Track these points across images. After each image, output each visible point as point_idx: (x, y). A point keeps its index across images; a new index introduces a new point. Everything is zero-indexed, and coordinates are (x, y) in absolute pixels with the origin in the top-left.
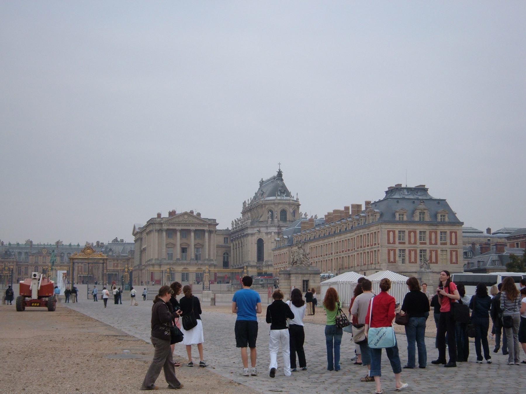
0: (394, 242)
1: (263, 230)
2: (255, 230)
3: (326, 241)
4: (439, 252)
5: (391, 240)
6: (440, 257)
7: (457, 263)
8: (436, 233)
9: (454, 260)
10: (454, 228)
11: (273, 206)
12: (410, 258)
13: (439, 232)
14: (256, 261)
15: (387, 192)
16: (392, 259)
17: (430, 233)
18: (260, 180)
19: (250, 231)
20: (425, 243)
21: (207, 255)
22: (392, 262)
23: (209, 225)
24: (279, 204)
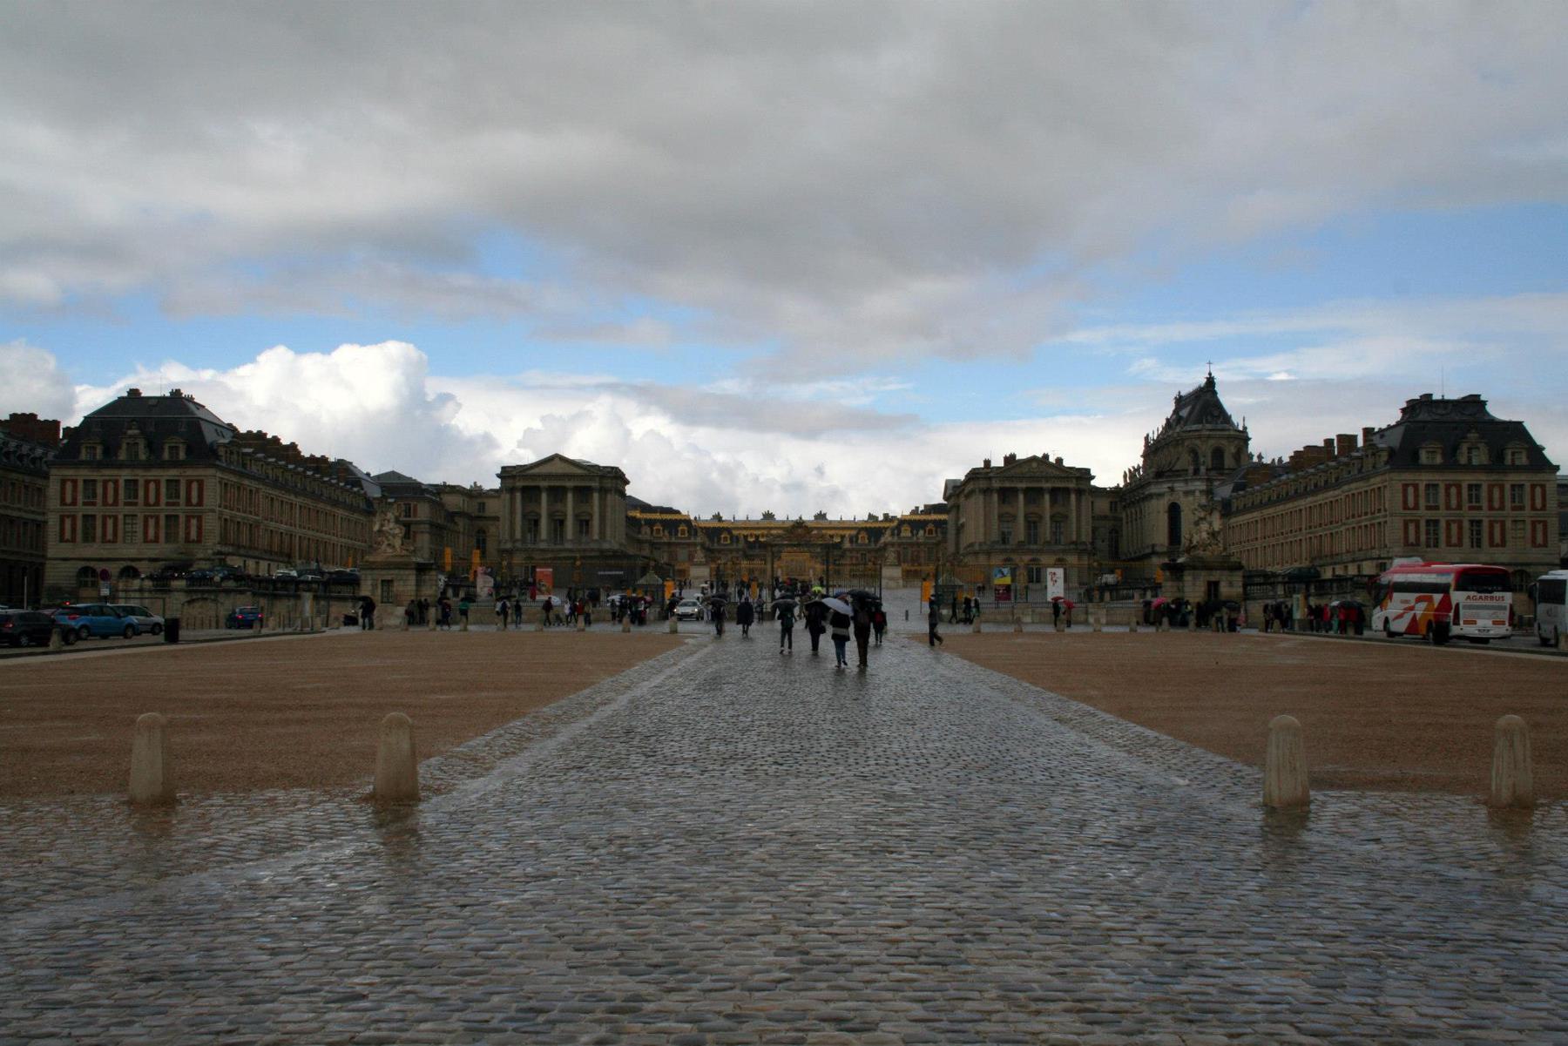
0: (1416, 507)
2: (1164, 488)
3: (1290, 505)
4: (1509, 524)
6: (1508, 537)
8: (1502, 488)
9: (1540, 539)
10: (1538, 477)
11: (1198, 442)
12: (1449, 536)
13: (1508, 487)
16: (1412, 539)
17: (1490, 488)
18: (1175, 394)
19: (1154, 489)
20: (1480, 508)
23: (1078, 479)
24: (1209, 437)
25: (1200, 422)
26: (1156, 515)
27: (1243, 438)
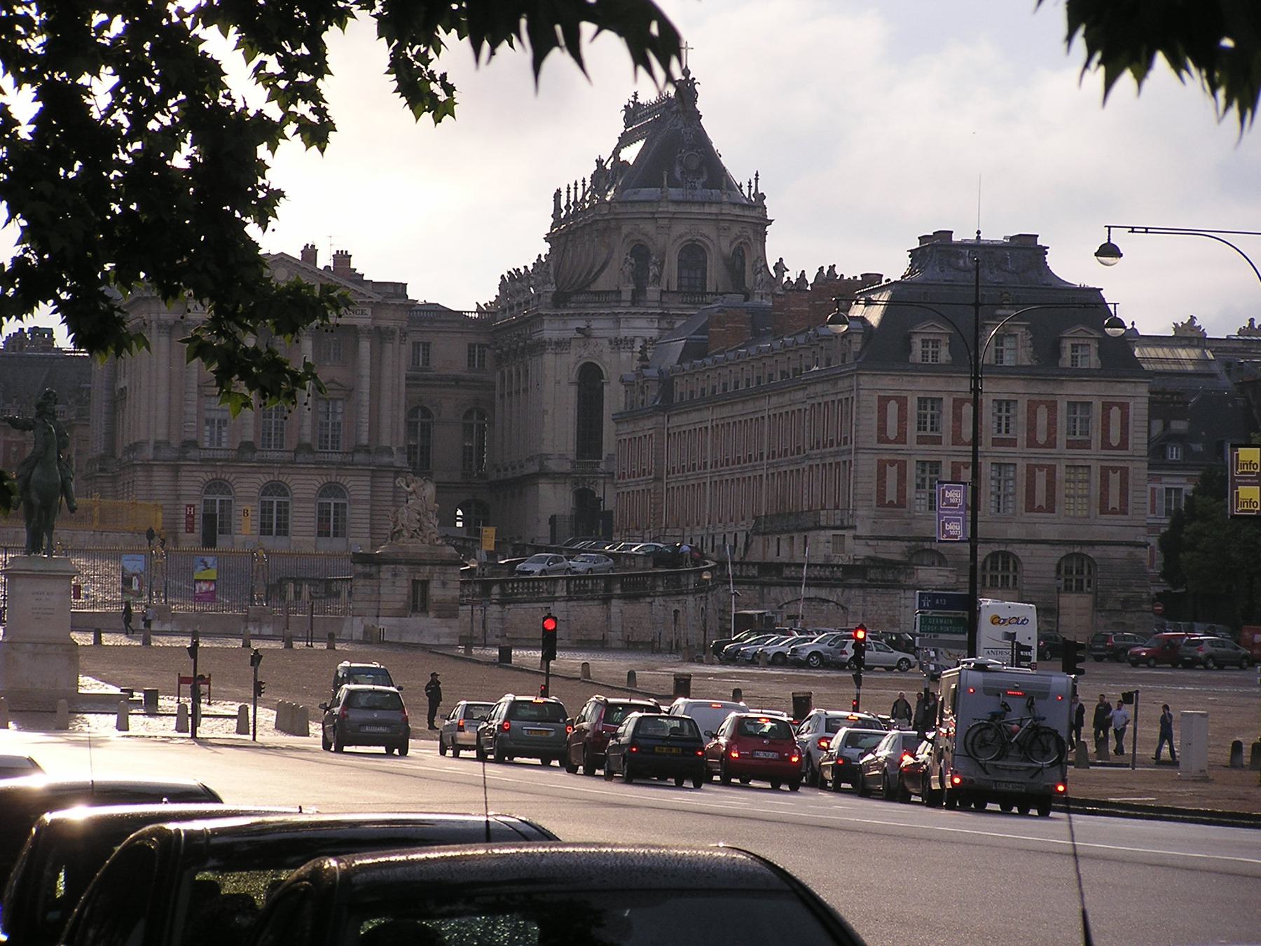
0: (901, 438)
1: (601, 327)
3: (750, 407)
4: (1061, 473)
5: (892, 432)
6: (1059, 495)
7: (1124, 512)
8: (1052, 407)
11: (649, 228)
13: (1062, 406)
14: (572, 456)
15: (913, 253)
16: (891, 496)
17: (1032, 407)
18: (626, 99)
21: (365, 428)
22: (891, 504)
24: (673, 218)
25: (657, 183)
26: (555, 379)
27: (752, 217)
